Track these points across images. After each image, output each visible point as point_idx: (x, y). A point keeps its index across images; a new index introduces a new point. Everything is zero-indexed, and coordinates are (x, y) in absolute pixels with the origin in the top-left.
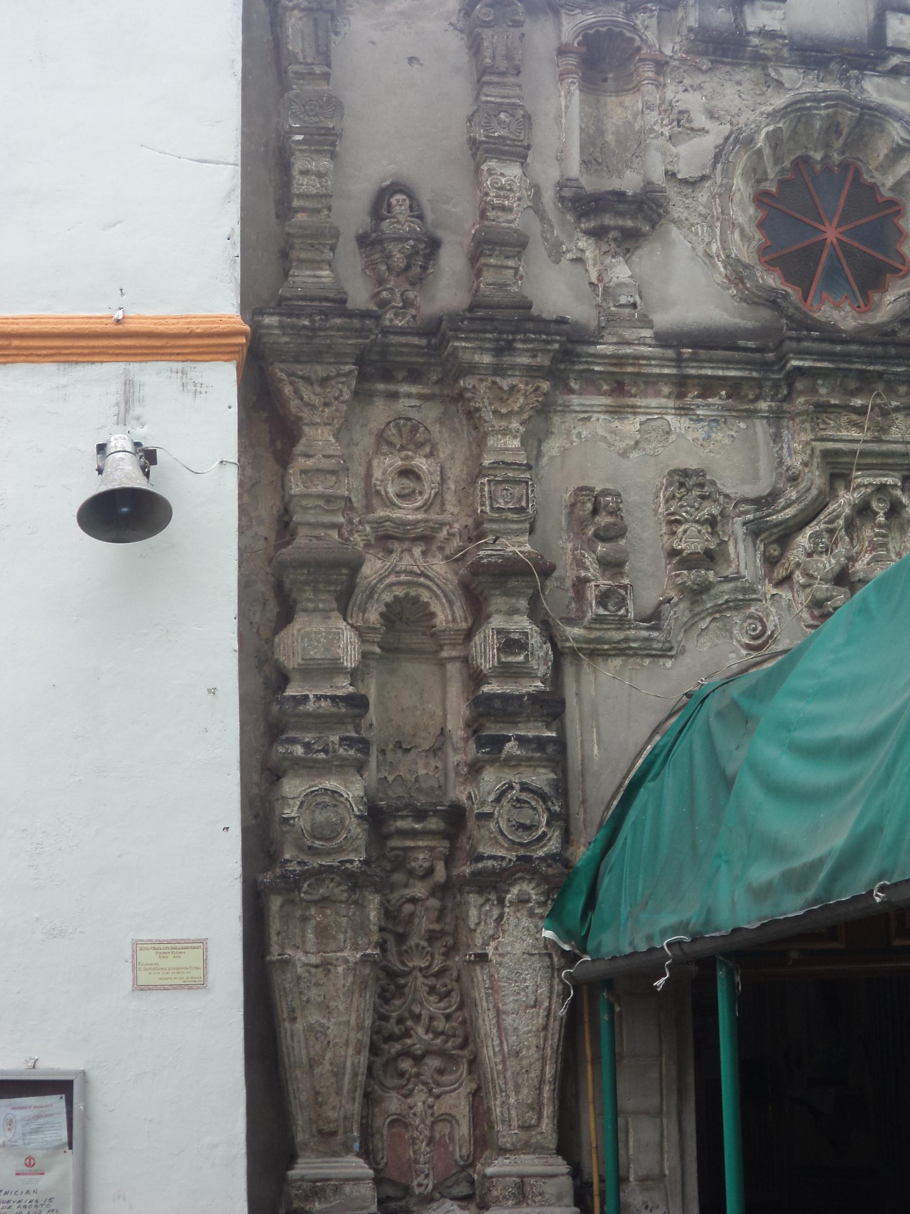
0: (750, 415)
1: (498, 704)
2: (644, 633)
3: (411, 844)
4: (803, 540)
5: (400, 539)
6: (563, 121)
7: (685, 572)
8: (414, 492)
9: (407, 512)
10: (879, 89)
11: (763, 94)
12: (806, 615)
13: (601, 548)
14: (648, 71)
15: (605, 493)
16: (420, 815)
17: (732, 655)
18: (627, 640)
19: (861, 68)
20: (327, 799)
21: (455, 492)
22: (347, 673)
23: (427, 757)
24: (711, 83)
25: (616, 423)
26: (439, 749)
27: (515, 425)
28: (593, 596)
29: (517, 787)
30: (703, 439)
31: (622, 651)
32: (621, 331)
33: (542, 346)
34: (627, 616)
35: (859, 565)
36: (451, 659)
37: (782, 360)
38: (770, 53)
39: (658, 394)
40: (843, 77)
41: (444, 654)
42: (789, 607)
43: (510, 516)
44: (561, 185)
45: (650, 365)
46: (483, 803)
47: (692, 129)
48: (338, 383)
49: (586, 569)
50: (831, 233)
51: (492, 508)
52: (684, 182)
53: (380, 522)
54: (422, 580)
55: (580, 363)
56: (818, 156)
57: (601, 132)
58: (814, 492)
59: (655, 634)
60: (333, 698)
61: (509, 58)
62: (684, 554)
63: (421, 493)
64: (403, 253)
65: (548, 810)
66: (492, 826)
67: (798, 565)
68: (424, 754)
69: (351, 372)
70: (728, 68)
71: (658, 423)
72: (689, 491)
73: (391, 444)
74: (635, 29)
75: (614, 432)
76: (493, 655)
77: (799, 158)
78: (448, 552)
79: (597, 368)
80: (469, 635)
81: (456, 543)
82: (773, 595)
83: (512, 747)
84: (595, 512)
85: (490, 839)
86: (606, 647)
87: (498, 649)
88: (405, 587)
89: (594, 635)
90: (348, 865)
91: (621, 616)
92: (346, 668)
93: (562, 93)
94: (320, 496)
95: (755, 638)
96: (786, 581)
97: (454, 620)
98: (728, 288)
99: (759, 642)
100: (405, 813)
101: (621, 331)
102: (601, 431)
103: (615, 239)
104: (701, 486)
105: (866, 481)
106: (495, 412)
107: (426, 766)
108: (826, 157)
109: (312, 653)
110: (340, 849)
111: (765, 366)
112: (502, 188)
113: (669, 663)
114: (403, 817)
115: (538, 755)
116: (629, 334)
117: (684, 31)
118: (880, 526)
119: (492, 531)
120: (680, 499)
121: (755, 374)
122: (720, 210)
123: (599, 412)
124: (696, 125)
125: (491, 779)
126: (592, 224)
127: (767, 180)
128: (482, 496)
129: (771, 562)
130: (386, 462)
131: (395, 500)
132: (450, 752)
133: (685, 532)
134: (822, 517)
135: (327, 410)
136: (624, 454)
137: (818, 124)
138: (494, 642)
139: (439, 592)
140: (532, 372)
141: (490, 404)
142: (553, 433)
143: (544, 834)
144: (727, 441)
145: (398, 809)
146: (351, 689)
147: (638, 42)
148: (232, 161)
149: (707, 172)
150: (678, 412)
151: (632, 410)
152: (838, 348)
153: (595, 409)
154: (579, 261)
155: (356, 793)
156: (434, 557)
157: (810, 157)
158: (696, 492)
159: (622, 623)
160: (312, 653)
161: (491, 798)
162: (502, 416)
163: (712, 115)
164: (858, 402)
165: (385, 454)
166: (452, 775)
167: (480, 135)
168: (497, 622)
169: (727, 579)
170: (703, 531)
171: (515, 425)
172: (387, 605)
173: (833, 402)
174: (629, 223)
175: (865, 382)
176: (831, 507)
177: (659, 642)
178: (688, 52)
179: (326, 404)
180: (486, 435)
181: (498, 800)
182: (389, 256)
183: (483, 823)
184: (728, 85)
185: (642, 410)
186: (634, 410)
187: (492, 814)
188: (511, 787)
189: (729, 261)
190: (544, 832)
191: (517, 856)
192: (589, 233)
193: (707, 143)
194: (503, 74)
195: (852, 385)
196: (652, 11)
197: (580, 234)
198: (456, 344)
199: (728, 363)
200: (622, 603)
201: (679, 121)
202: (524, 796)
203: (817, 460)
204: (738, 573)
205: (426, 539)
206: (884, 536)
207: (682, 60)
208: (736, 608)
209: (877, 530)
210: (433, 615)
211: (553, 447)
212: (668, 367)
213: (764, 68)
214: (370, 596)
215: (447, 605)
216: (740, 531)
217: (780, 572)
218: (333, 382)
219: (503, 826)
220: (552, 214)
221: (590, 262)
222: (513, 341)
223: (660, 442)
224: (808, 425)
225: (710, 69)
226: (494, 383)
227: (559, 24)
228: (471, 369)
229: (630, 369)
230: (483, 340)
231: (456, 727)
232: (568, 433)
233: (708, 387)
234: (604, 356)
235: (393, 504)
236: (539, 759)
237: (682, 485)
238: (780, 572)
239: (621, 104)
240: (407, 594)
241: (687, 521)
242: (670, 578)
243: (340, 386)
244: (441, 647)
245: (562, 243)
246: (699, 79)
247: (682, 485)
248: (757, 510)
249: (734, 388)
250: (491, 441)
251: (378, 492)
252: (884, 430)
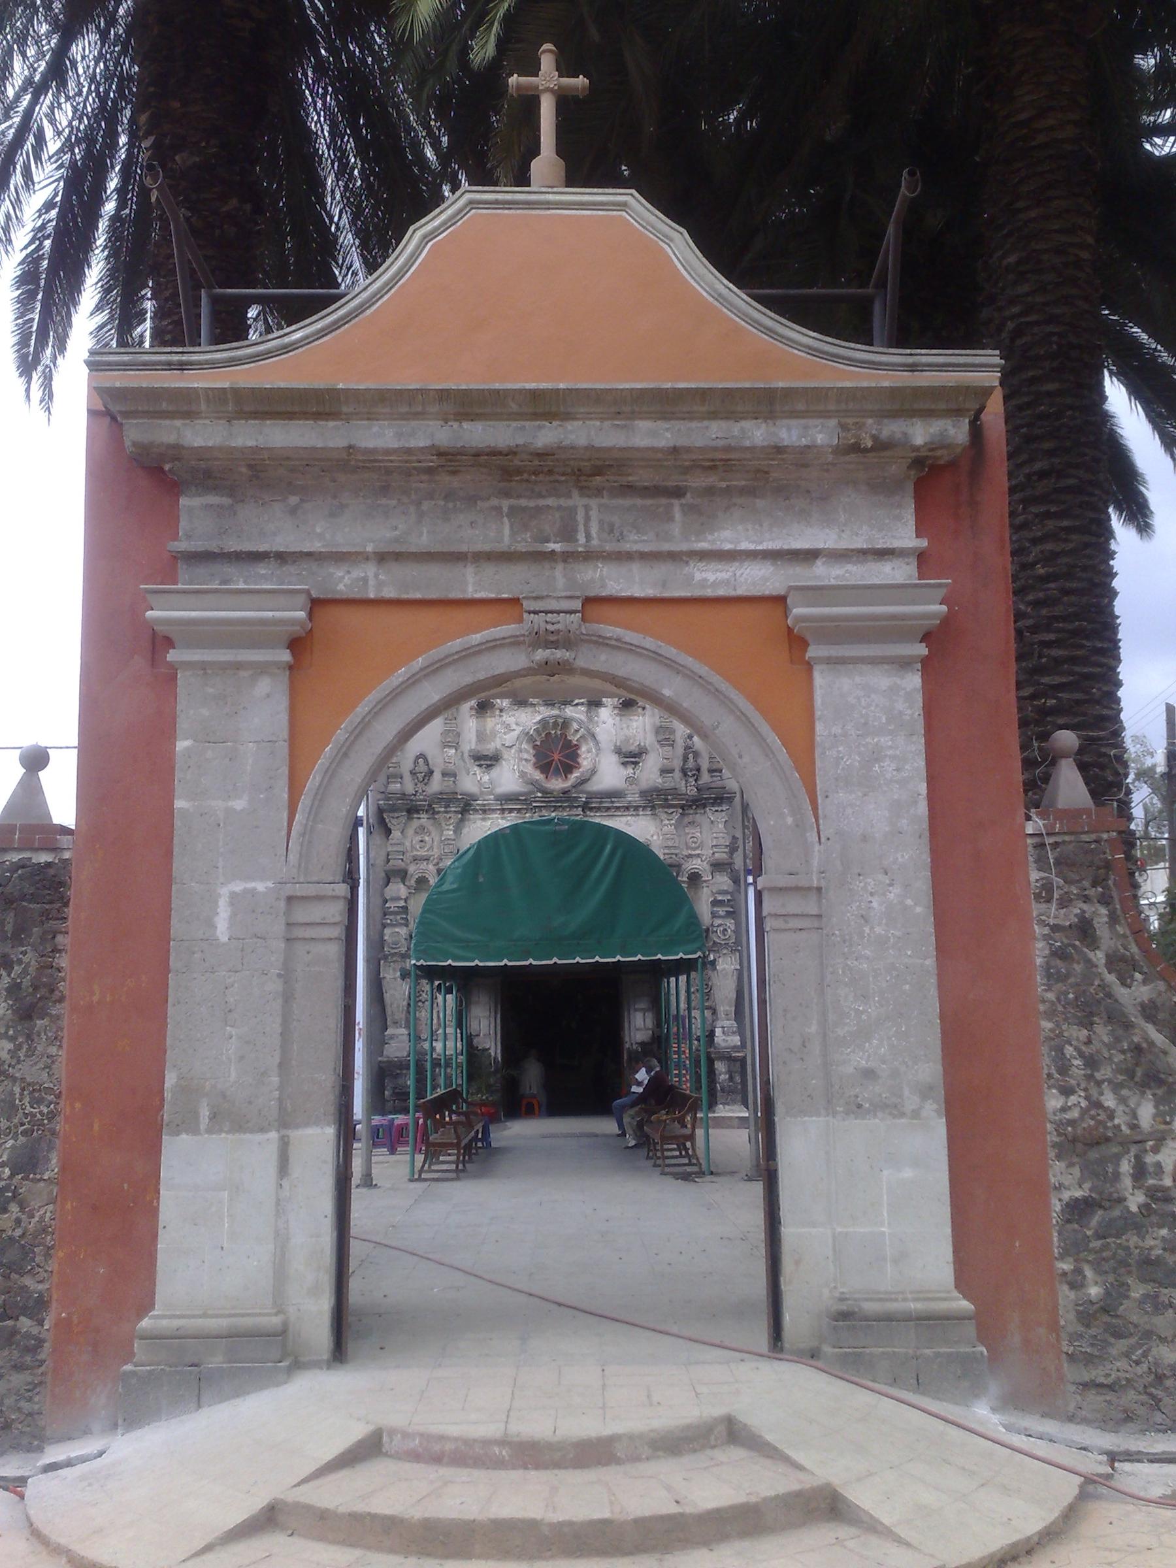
9: (422, 853)
10: (571, 711)
14: (497, 712)
24: (517, 714)
27: (451, 827)
40: (560, 708)
50: (556, 757)
57: (485, 730)
81: (435, 861)
116: (487, 798)
154: (475, 774)
163: (517, 724)
171: (451, 827)
174: (489, 763)
193: (515, 734)
199: (516, 804)
205: (428, 860)
211: (465, 831)
220: (467, 761)
228: (439, 812)
246: (514, 712)
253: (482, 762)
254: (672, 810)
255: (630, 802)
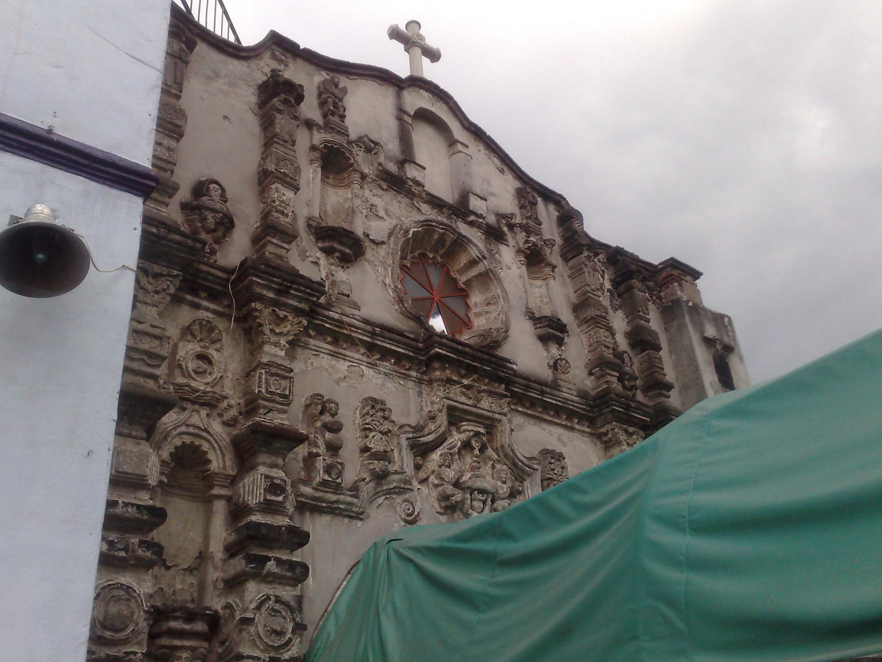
0: (406, 377)
1: (264, 531)
2: (349, 499)
3: (177, 642)
4: (436, 456)
5: (193, 402)
6: (311, 185)
7: (376, 461)
8: (205, 372)
9: (199, 384)
11: (411, 212)
12: (436, 505)
13: (328, 435)
14: (357, 176)
15: (331, 401)
16: (191, 617)
17: (396, 525)
18: (337, 502)
19: (458, 216)
20: (122, 593)
21: (232, 380)
22: (149, 490)
23: (184, 574)
25: (334, 362)
26: (195, 569)
27: (283, 342)
28: (322, 466)
29: (273, 598)
30: (381, 385)
31: (332, 510)
32: (343, 307)
33: (306, 297)
34: (341, 484)
35: (464, 478)
36: (219, 497)
37: (428, 347)
38: (417, 192)
39: (358, 351)
41: (216, 491)
42: (427, 498)
43: (278, 399)
44: (310, 219)
45: (357, 332)
46: (245, 610)
47: (378, 216)
48: (167, 280)
49: (317, 446)
51: (267, 391)
52: (372, 241)
53: (180, 386)
54: (204, 434)
55: (318, 319)
56: (431, 256)
58: (443, 429)
59: (355, 500)
60: (139, 507)
61: (291, 136)
62: (372, 451)
63: (210, 374)
64: (215, 220)
65: (294, 619)
66: (252, 629)
67: (433, 472)
68: (182, 572)
69: (178, 276)
70: (395, 193)
71: (356, 369)
72: (377, 412)
73: (194, 337)
74: (351, 153)
75: (332, 367)
76: (260, 494)
77: (421, 253)
78: (225, 418)
79: (327, 325)
80: (233, 481)
81: (233, 412)
82: (418, 489)
83: (273, 565)
84: (322, 413)
85: (249, 641)
86: (324, 505)
87: (265, 489)
88: (191, 437)
89: (319, 494)
90: (132, 657)
91: (338, 483)
92: (149, 484)
93: (311, 171)
94: (146, 352)
95: (409, 515)
96: (424, 481)
97: (225, 467)
98: (394, 305)
99: (410, 518)
100: (178, 614)
101: (343, 307)
102: (325, 364)
103: (338, 258)
104: (384, 410)
105: (470, 428)
106: (272, 330)
107: (183, 582)
108: (434, 257)
109: (125, 467)
110: (126, 641)
111: (416, 350)
112: (283, 202)
113: (359, 524)
114: (175, 619)
115: (289, 574)
117: (376, 165)
118: (477, 456)
119: (265, 407)
120: (372, 416)
121: (411, 354)
122: (391, 261)
123: (324, 353)
124: (380, 215)
125: (253, 591)
126: (327, 244)
127: (406, 259)
128: (260, 381)
129: (418, 467)
130: (189, 346)
131: (192, 373)
132: (211, 569)
133: (373, 437)
134: (445, 444)
135: (155, 295)
136: (338, 382)
137: (436, 237)
138: (263, 484)
139: (216, 445)
140: (298, 312)
141: (269, 324)
142: (296, 359)
143: (290, 640)
144: (394, 389)
145: (174, 610)
146: (151, 502)
147: (352, 161)
148: (159, 69)
149: (385, 240)
150: (368, 365)
151: (342, 357)
152: (460, 347)
153: (322, 350)
154: (316, 263)
155: (146, 591)
156: (214, 420)
157: (427, 255)
158: (379, 414)
159: (337, 488)
160: (125, 467)
161: (253, 606)
162: (276, 334)
163: (386, 211)
164: (466, 382)
165: (189, 341)
166: (210, 589)
167: (271, 167)
168: (262, 469)
169: (396, 473)
170: (384, 439)
172: (176, 448)
173: (454, 378)
174: (348, 251)
175: (471, 370)
176: (450, 440)
177: (357, 506)
178: (376, 176)
179: (157, 292)
180: (263, 343)
181: (258, 608)
182: (203, 219)
183: (244, 627)
184: (394, 201)
185: (349, 358)
186: (344, 357)
187: (253, 619)
188: (268, 598)
189: (395, 289)
190: (289, 638)
191: (269, 657)
192: (323, 250)
194: (285, 141)
195: (463, 372)
196: (361, 148)
197: (317, 249)
198: (254, 278)
199: (398, 343)
200: (340, 474)
201: (371, 209)
202: (277, 607)
203: (445, 410)
204: (402, 468)
206: (479, 463)
207: (374, 181)
208: (398, 493)
209: (474, 459)
210: (209, 462)
212: (366, 336)
213: (412, 200)
214: (165, 438)
215: (220, 456)
216: (404, 443)
217: (422, 475)
218: (163, 279)
219: (261, 630)
221: (322, 267)
222: (290, 288)
223: (357, 380)
224: (442, 389)
225: (386, 190)
226: (274, 311)
227: (312, 134)
228: (261, 298)
229: (345, 332)
230: (272, 281)
231: (216, 548)
232: (306, 362)
233: (386, 354)
234: (333, 319)
235: (190, 376)
236: (289, 578)
237: (373, 407)
238: (422, 475)
239: (336, 193)
240: (192, 442)
241: (375, 430)
242: (362, 465)
243: (169, 283)
244: (211, 487)
245: (307, 251)
246: (381, 192)
247: (373, 407)
248: (413, 432)
249: (399, 358)
250: (267, 348)
251: (180, 366)
252: (479, 401)
253: (336, 245)
254: (631, 429)
255: (565, 399)
